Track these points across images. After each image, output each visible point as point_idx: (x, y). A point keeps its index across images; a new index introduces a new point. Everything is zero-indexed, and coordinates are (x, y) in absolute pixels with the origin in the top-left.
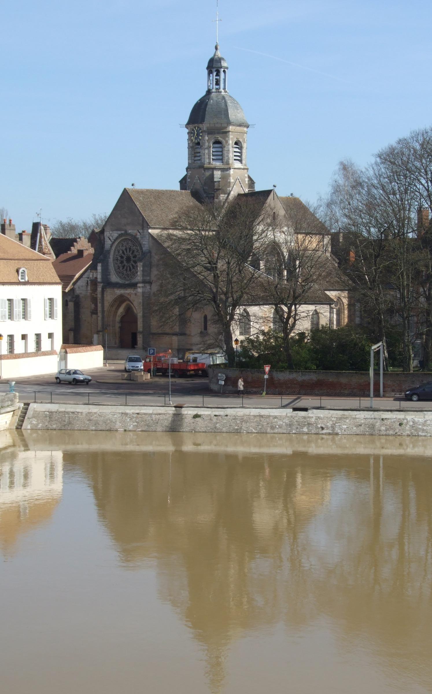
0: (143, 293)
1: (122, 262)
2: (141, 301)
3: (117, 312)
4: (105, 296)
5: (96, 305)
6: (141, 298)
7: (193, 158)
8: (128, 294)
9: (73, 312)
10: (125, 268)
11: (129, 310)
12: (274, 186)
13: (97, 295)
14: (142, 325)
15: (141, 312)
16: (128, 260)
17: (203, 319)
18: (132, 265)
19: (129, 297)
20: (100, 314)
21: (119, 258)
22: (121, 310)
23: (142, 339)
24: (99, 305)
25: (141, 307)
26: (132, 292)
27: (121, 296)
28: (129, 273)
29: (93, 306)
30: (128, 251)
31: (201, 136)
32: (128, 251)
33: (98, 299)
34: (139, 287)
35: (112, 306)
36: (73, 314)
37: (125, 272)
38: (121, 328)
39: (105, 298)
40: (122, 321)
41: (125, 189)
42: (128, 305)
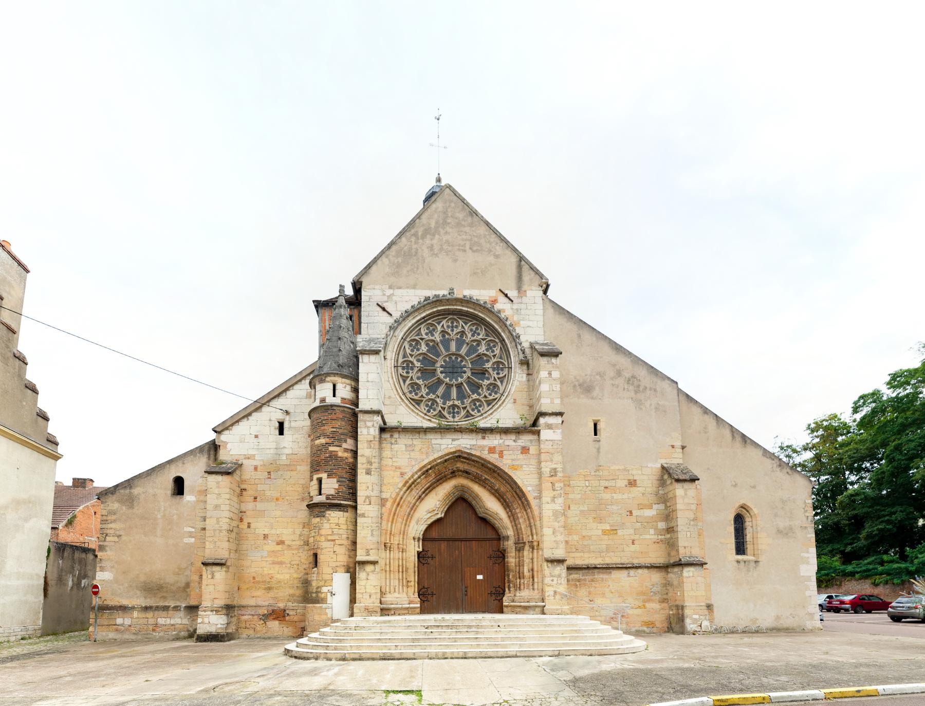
8: (492, 450)
19: (493, 458)
40: (426, 538)
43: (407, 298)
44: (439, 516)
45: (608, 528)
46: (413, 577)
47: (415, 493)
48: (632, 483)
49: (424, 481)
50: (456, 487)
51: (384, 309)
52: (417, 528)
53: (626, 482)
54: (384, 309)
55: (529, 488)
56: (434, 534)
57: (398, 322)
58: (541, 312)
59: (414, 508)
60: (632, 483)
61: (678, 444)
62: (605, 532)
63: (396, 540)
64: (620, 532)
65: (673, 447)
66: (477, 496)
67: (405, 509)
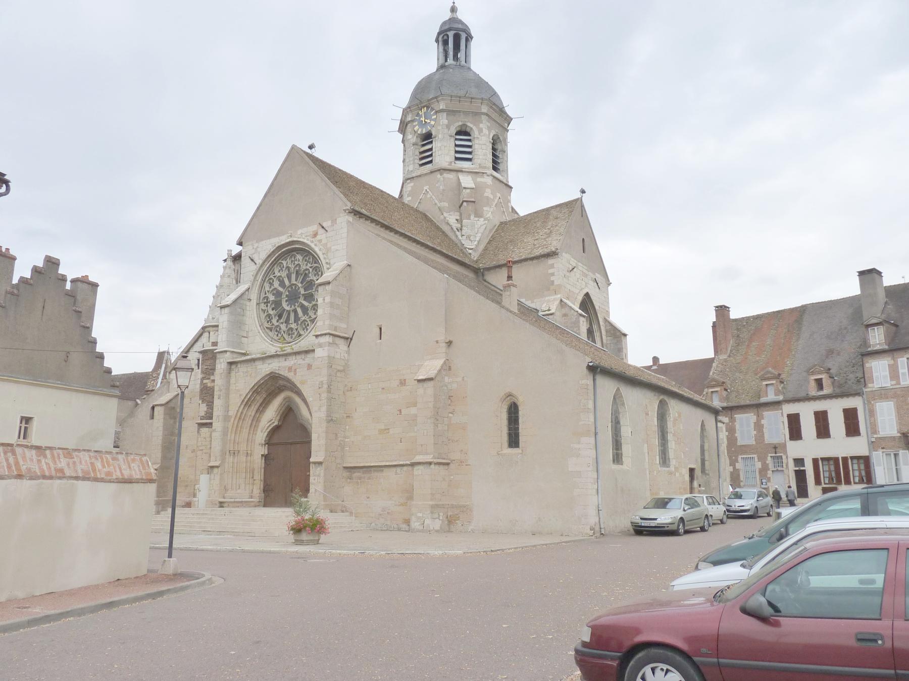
0: (331, 359)
1: (277, 304)
2: (325, 379)
3: (258, 421)
4: (233, 381)
5: (210, 405)
6: (325, 371)
7: (417, 161)
8: (290, 369)
9: (161, 428)
10: (285, 316)
11: (288, 413)
12: (583, 192)
13: (213, 381)
14: (323, 442)
15: (324, 409)
16: (293, 297)
17: (504, 416)
18: (302, 306)
19: (290, 375)
20: (217, 424)
21: (272, 298)
22: (271, 415)
23: (321, 480)
24: (218, 403)
25: (324, 395)
26: (301, 362)
27: (273, 377)
28: (294, 326)
29: (204, 408)
30: (293, 276)
31: (435, 120)
32: (293, 276)
33: (216, 389)
34: (320, 345)
35: (247, 403)
36: (161, 433)
37: (283, 327)
38: (266, 457)
39: (232, 387)
41: (294, 148)
42: (288, 400)
43: (267, 246)
44: (276, 423)
45: (383, 427)
46: (259, 476)
47: (254, 408)
48: (403, 383)
49: (258, 398)
50: (285, 399)
51: (252, 260)
52: (261, 436)
53: (397, 382)
54: (252, 260)
55: (311, 399)
56: (275, 440)
57: (261, 266)
58: (345, 235)
59: (256, 420)
60: (403, 383)
61: (442, 338)
62: (381, 432)
63: (243, 447)
64: (391, 432)
65: (437, 342)
66: (297, 407)
67: (248, 421)
